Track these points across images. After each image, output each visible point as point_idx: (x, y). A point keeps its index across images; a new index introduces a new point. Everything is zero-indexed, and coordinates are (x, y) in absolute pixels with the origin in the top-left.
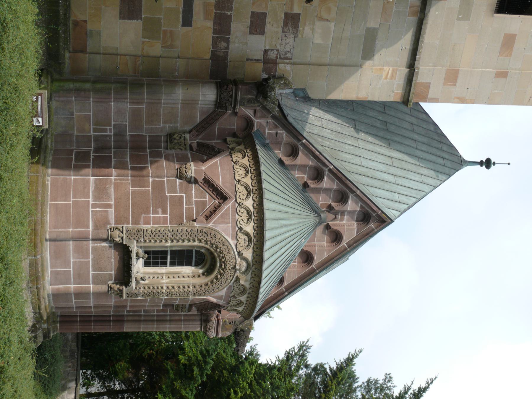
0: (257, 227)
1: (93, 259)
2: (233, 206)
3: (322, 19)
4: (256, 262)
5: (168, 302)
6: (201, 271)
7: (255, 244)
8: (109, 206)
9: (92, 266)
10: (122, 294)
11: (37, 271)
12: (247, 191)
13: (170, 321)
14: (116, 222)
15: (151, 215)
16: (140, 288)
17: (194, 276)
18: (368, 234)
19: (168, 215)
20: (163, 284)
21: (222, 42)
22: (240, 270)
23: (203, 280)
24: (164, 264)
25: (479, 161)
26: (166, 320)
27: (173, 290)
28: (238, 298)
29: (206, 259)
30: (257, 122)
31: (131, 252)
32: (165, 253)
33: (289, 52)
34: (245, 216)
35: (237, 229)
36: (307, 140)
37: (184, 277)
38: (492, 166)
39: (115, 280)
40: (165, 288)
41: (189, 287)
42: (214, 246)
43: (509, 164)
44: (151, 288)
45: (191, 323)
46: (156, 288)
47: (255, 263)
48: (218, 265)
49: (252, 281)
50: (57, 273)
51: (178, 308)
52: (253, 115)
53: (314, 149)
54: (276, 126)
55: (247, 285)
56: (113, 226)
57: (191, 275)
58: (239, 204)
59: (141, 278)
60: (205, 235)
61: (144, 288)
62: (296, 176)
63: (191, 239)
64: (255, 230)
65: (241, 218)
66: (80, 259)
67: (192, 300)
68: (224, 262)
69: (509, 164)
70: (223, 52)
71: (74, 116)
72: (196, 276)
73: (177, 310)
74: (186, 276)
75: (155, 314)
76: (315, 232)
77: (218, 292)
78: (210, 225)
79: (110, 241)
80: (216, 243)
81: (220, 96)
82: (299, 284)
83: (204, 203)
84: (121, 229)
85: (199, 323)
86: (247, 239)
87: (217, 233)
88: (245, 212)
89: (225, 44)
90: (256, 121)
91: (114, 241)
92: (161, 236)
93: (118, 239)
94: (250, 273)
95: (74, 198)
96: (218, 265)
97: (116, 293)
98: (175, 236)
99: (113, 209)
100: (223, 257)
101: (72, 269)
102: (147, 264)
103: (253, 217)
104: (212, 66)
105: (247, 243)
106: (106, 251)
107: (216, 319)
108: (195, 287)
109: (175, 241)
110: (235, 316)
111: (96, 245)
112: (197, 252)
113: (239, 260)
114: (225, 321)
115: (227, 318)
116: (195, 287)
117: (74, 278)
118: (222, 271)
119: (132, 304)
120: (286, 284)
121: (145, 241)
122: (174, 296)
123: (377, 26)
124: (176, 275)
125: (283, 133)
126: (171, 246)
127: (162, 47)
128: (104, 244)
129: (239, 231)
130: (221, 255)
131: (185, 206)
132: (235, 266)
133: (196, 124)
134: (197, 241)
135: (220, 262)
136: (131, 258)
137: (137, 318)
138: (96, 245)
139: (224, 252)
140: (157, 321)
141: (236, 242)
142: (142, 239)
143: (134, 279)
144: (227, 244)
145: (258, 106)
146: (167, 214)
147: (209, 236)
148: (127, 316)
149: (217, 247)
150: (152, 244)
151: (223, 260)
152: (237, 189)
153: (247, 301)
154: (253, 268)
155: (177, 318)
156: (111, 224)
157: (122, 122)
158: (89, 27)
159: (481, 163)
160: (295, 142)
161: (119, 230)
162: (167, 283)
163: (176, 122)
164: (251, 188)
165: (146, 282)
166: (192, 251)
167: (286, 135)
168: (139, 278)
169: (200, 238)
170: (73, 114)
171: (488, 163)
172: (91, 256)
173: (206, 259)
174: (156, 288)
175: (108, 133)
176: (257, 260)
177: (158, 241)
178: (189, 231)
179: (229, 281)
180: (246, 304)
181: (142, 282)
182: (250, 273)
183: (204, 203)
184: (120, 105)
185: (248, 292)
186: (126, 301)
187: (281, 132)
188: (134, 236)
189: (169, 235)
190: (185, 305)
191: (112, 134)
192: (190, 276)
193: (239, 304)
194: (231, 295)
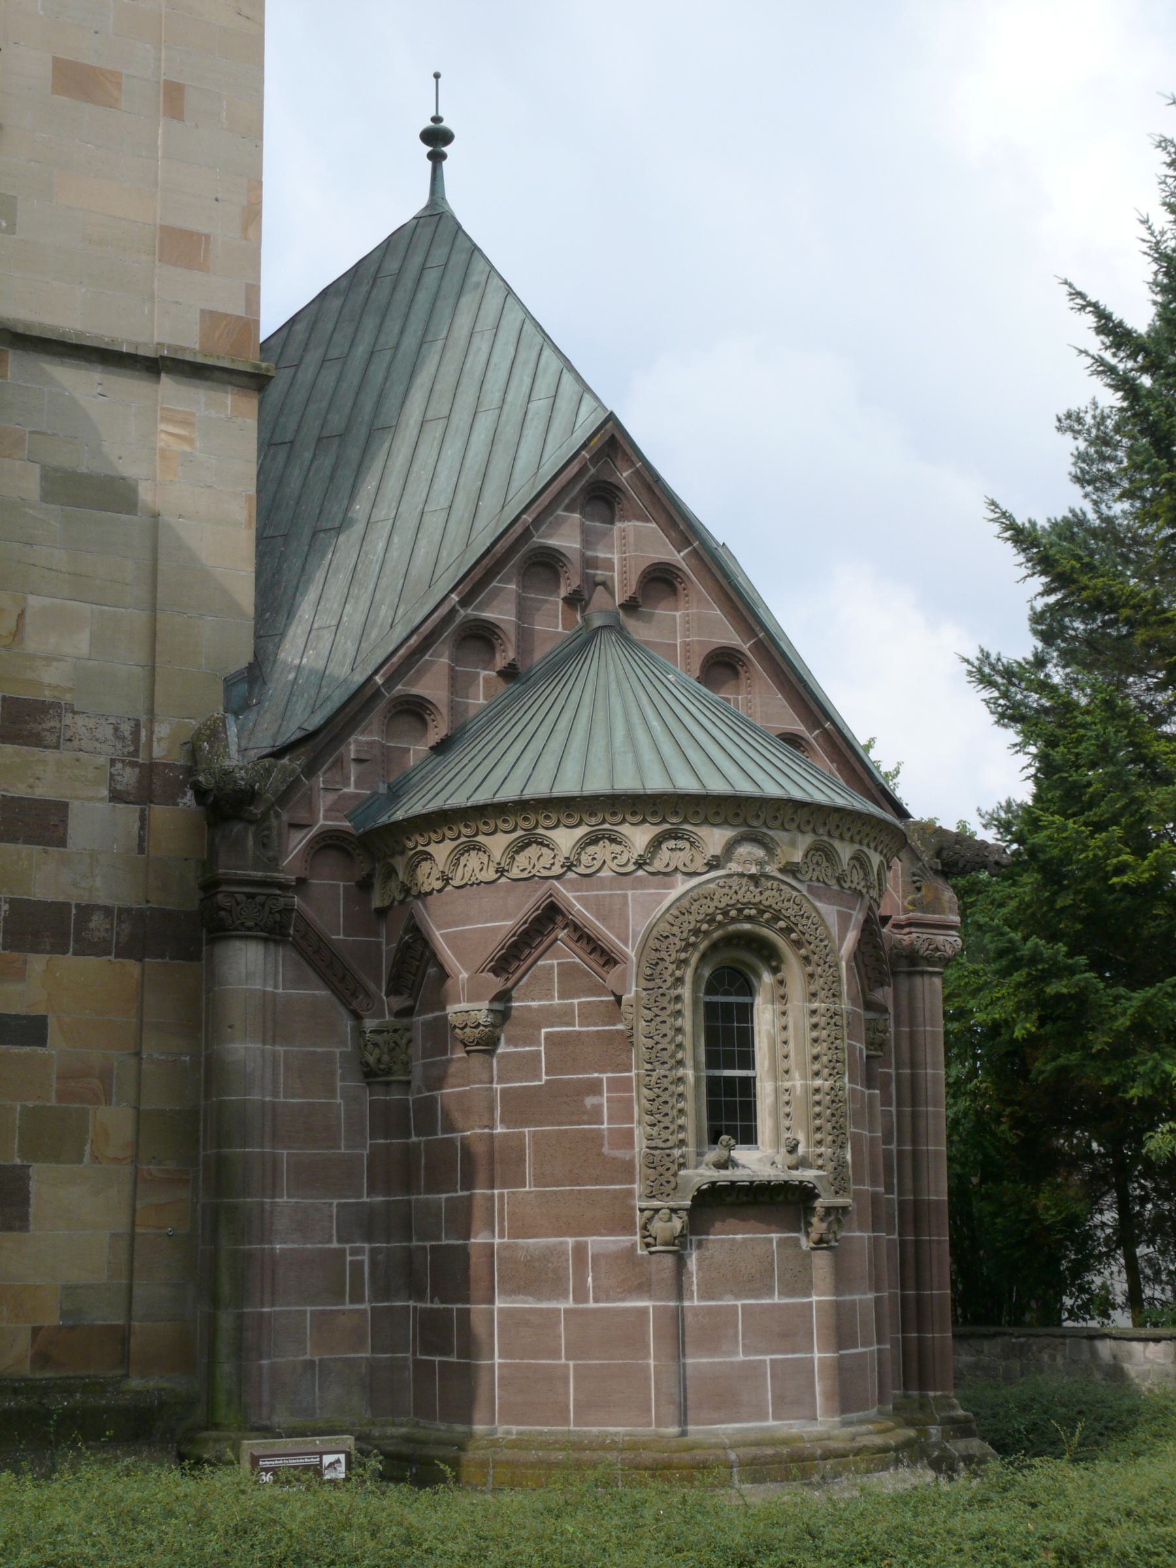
0: (634, 814)
1: (738, 1296)
3: (18, 633)
4: (737, 815)
5: (860, 1073)
6: (767, 978)
7: (686, 821)
8: (580, 1250)
10: (837, 1208)
11: (776, 1459)
12: (529, 844)
13: (913, 1065)
14: (628, 1229)
15: (605, 1126)
16: (820, 1155)
17: (783, 997)
18: (650, 489)
19: (604, 1076)
20: (806, 1088)
21: (92, 925)
22: (760, 863)
23: (794, 970)
24: (748, 1085)
25: (430, 163)
26: (914, 1078)
27: (825, 1059)
28: (845, 867)
29: (732, 962)
30: (325, 818)
31: (713, 1183)
32: (714, 1085)
33: (116, 729)
34: (602, 851)
35: (640, 873)
36: (376, 672)
37: (785, 1028)
38: (444, 124)
39: (798, 1230)
40: (818, 1082)
41: (814, 1012)
42: (692, 939)
43: (437, 76)
44: (818, 1122)
45: (920, 1005)
46: (817, 1109)
48: (747, 926)
49: (794, 825)
50: (779, 1399)
51: (876, 1044)
52: (306, 831)
53: (402, 652)
55: (805, 841)
56: (638, 1238)
57: (778, 1007)
58: (569, 868)
59: (790, 1152)
60: (660, 967)
61: (820, 1142)
62: (482, 701)
63: (671, 1007)
64: (644, 821)
65: (609, 862)
66: (737, 1333)
67: (853, 1001)
68: (740, 911)
69: (437, 76)
70: (120, 921)
71: (316, 1359)
72: (781, 991)
73: (881, 1045)
74: (783, 1021)
75: (893, 1109)
76: (647, 643)
77: (826, 927)
78: (631, 952)
79: (683, 1246)
80: (685, 935)
81: (249, 929)
82: (801, 690)
83: (568, 971)
84: (647, 1214)
85: (918, 980)
86: (671, 844)
87: (654, 933)
88: (591, 849)
89: (95, 917)
90: (321, 822)
91: (682, 1235)
92: (665, 1096)
93: (677, 1224)
94: (771, 833)
95: (555, 1354)
96: (747, 926)
97: (835, 1227)
98: (665, 1056)
99: (589, 1239)
100: (725, 913)
101: (768, 1358)
102: (748, 1137)
103: (606, 826)
104: (163, 956)
105: (681, 844)
106: (712, 1256)
107: (907, 930)
108: (814, 995)
109: (679, 1056)
110: (896, 876)
111: (695, 1288)
112: (708, 992)
113: (734, 867)
114: (913, 903)
115: (904, 897)
116: (814, 995)
117: (793, 1352)
118: (767, 915)
119: (867, 1180)
120: (799, 728)
121: (682, 1143)
122: (840, 1056)
123: (37, 469)
124: (781, 1050)
125: (356, 741)
126: (696, 1067)
127: (108, 1102)
128: (693, 1263)
129: (647, 868)
130: (719, 918)
131: (577, 1028)
132: (752, 877)
133: (334, 999)
134: (679, 991)
135: (740, 921)
136: (733, 1183)
138: (695, 1288)
139: (711, 911)
140: (914, 1103)
141: (679, 876)
142: (676, 1152)
143: (794, 1172)
144: (685, 903)
145: (278, 816)
146: (601, 1080)
147: (663, 954)
148: (900, 1193)
149: (696, 932)
150: (688, 1121)
151: (733, 913)
152: (525, 875)
153: (852, 840)
154: (754, 823)
155: (905, 1046)
156: (634, 1245)
157: (331, 1217)
158: (52, 1320)
159: (437, 158)
160: (381, 705)
161: (650, 1219)
162: (804, 1077)
164: (519, 833)
165: (801, 1137)
166: (707, 1004)
167: (362, 733)
168: (792, 1160)
169: (670, 980)
170: (311, 1363)
171: (437, 138)
173: (732, 962)
174: (817, 1109)
175: (366, 1258)
177: (680, 1106)
178: (648, 1014)
179: (795, 893)
180: (861, 843)
181: (801, 1149)
182: (771, 833)
183: (568, 971)
185: (825, 838)
186: (857, 1196)
187: (352, 747)
188: (668, 1174)
189: (663, 1072)
190: (868, 1021)
191: (367, 1246)
192: (783, 1008)
193: (862, 865)
194: (836, 887)
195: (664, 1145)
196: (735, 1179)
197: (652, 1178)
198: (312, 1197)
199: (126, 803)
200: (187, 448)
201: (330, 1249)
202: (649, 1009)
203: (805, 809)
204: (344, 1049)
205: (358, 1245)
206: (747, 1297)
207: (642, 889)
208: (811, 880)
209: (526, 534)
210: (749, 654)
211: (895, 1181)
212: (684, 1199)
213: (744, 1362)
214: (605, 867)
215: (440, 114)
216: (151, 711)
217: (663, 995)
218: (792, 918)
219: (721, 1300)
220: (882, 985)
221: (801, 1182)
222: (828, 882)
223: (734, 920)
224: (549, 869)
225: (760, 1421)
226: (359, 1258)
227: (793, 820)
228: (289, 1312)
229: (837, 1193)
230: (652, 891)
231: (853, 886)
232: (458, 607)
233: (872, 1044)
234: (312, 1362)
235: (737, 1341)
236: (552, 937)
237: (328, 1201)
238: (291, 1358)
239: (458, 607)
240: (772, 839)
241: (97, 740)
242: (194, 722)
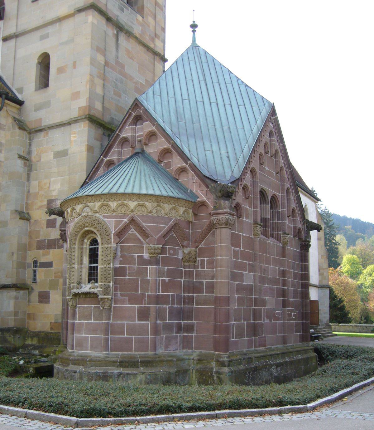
3: (49, 187)
11: (78, 360)
25: (192, 33)
42: (76, 233)
50: (91, 346)
100: (82, 226)
120: (184, 164)
123: (53, 152)
158: (53, 321)
159: (194, 31)
171: (194, 26)
200: (75, 139)
223: (84, 227)
239: (104, 158)
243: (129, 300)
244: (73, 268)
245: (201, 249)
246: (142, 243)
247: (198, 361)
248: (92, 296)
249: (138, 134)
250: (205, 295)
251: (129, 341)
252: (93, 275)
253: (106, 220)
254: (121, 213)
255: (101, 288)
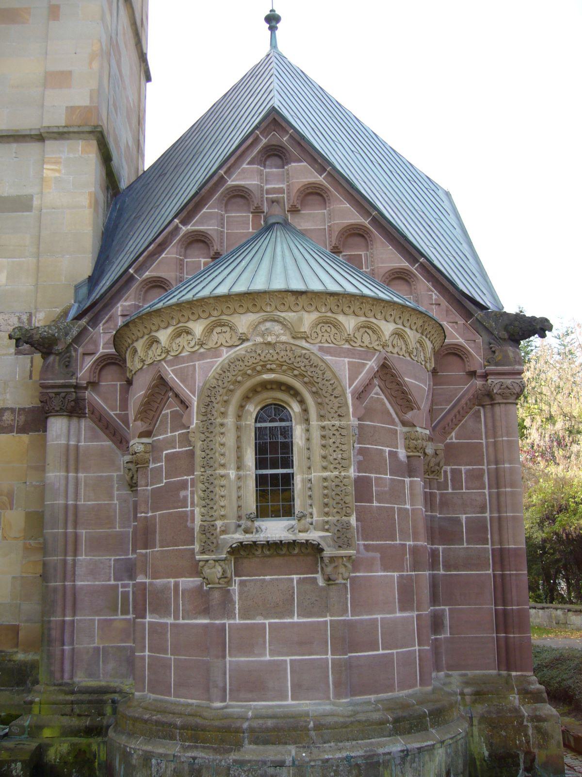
1: (266, 618)
2: (171, 363)
7: (222, 313)
8: (176, 585)
9: (280, 618)
11: (276, 729)
18: (299, 144)
21: (4, 418)
25: (269, 32)
30: (103, 348)
31: (241, 543)
33: (19, 319)
34: (183, 340)
35: (202, 350)
36: (130, 267)
38: (277, 12)
47: (258, 308)
52: (93, 356)
53: (145, 254)
54: (110, 317)
64: (199, 317)
66: (265, 642)
70: (19, 414)
71: (101, 646)
75: (486, 491)
76: (306, 230)
81: (57, 411)
82: (402, 241)
85: (497, 409)
86: (218, 329)
88: (177, 341)
89: (6, 414)
90: (101, 351)
94: (283, 314)
95: (165, 651)
100: (254, 369)
101: (288, 658)
103: (181, 325)
104: (39, 431)
105: (224, 329)
111: (237, 611)
117: (310, 654)
120: (405, 264)
125: (121, 305)
127: (11, 509)
131: (177, 450)
133: (114, 446)
136: (255, 542)
137: (496, 525)
138: (237, 611)
145: (76, 350)
148: (492, 544)
154: (269, 309)
157: (110, 566)
159: (273, 29)
160: (135, 286)
163: (110, 479)
167: (126, 300)
170: (97, 649)
171: (272, 20)
172: (259, 621)
175: (130, 589)
176: (250, 306)
178: (203, 437)
179: (304, 352)
184: (79, 571)
185: (329, 314)
187: (120, 309)
191: (131, 582)
195: (210, 519)
196: (254, 540)
197: (204, 541)
198: (99, 556)
199: (24, 354)
200: (57, 175)
201: (110, 585)
202: (204, 433)
203: (304, 297)
204: (118, 473)
205: (126, 582)
206: (273, 618)
207: (203, 360)
208: (321, 342)
209: (222, 180)
210: (369, 226)
211: (489, 536)
212: (221, 553)
213: (269, 661)
214: (185, 350)
215: (274, 9)
216: (36, 309)
217: (211, 424)
218: (302, 368)
219: (255, 619)
220: (412, 410)
221: (307, 541)
222: (337, 343)
224: (160, 355)
225: (281, 700)
226: (126, 589)
227: (408, 320)
228: (85, 620)
229: (340, 547)
230: (209, 360)
231: (364, 345)
232: (180, 226)
233: (409, 448)
234: (98, 648)
235: (265, 648)
236: (167, 397)
237: (108, 557)
238: (85, 645)
239: (180, 226)
240: (284, 318)
241: (9, 325)
242: (58, 310)
243: (382, 558)
244: (222, 476)
245: (449, 447)
246: (393, 423)
247: (473, 697)
248: (296, 551)
249: (269, 186)
250: (465, 545)
251: (386, 662)
252: (275, 494)
253: (328, 358)
254: (362, 344)
255: (327, 530)
